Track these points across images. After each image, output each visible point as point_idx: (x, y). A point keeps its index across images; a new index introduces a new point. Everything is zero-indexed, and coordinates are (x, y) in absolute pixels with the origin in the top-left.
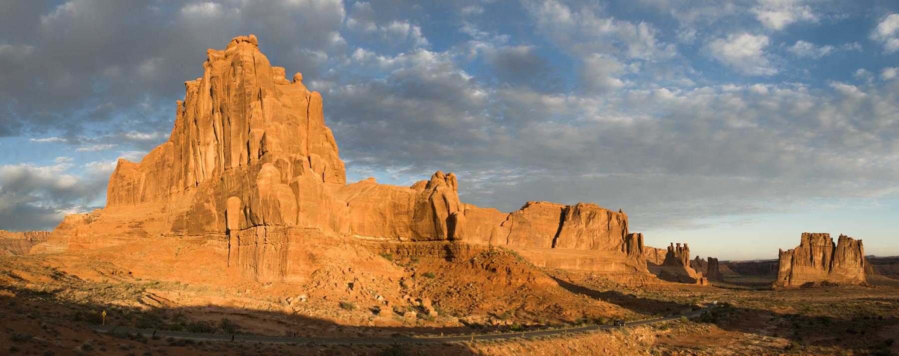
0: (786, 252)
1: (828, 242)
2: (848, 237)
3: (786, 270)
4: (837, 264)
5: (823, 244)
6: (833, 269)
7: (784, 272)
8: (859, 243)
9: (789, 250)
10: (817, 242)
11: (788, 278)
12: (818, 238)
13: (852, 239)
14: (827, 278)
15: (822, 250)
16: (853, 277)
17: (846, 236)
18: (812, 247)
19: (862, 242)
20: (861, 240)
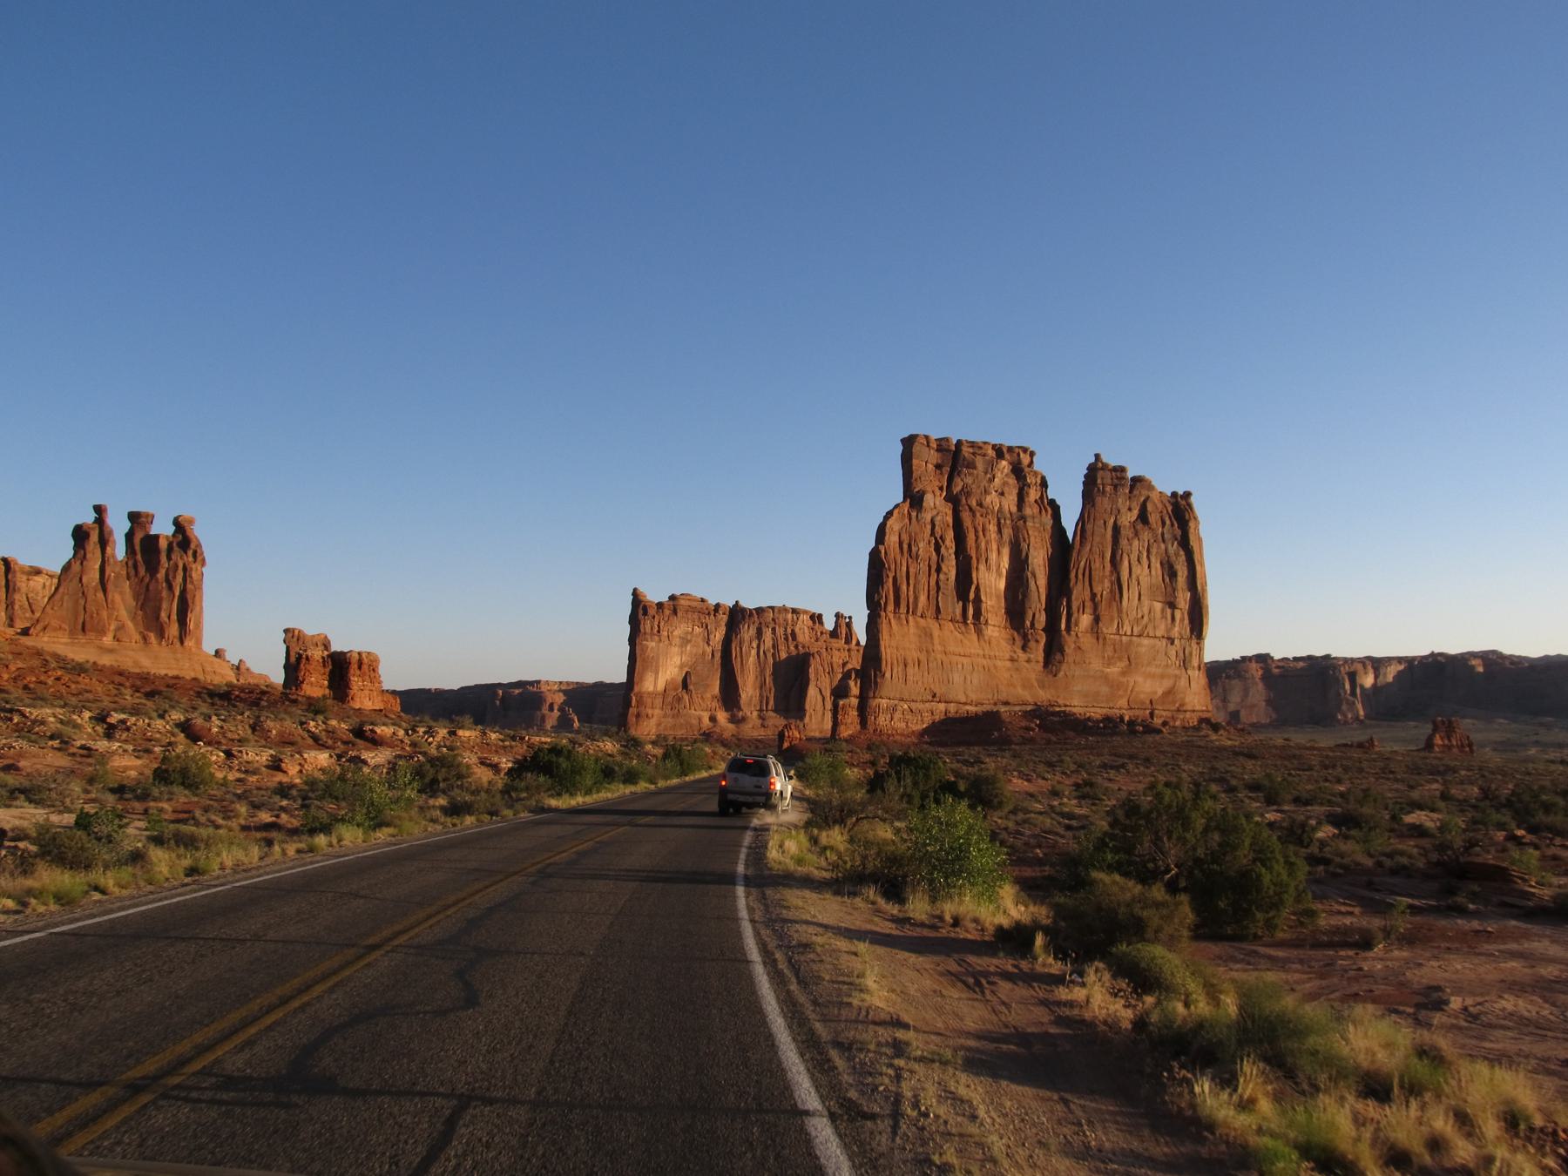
0: (660, 605)
1: (1033, 495)
2: (1130, 474)
3: (661, 686)
4: (1085, 620)
5: (1010, 502)
6: (1069, 643)
7: (654, 695)
8: (1180, 509)
9: (672, 598)
10: (986, 492)
11: (855, 689)
12: (991, 467)
13: (1151, 487)
14: (1043, 696)
15: (1007, 532)
16: (1160, 692)
17: (1122, 469)
18: (966, 516)
19: (1193, 499)
20: (1187, 495)
